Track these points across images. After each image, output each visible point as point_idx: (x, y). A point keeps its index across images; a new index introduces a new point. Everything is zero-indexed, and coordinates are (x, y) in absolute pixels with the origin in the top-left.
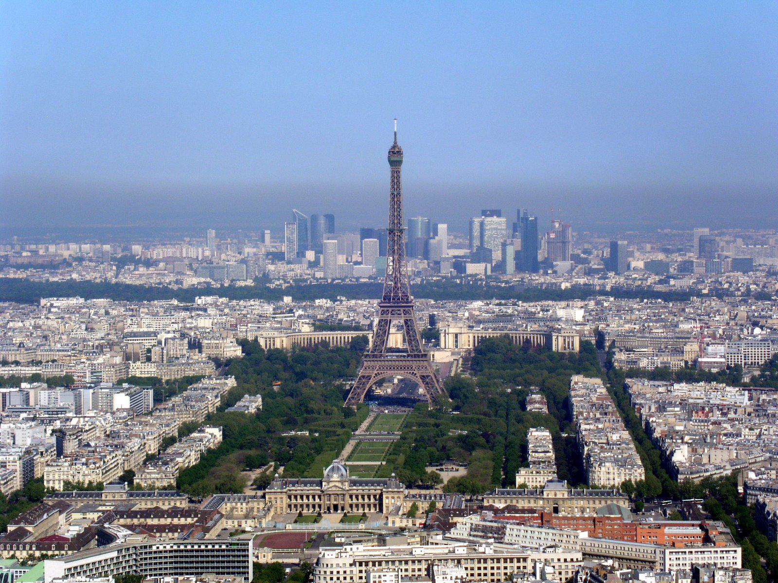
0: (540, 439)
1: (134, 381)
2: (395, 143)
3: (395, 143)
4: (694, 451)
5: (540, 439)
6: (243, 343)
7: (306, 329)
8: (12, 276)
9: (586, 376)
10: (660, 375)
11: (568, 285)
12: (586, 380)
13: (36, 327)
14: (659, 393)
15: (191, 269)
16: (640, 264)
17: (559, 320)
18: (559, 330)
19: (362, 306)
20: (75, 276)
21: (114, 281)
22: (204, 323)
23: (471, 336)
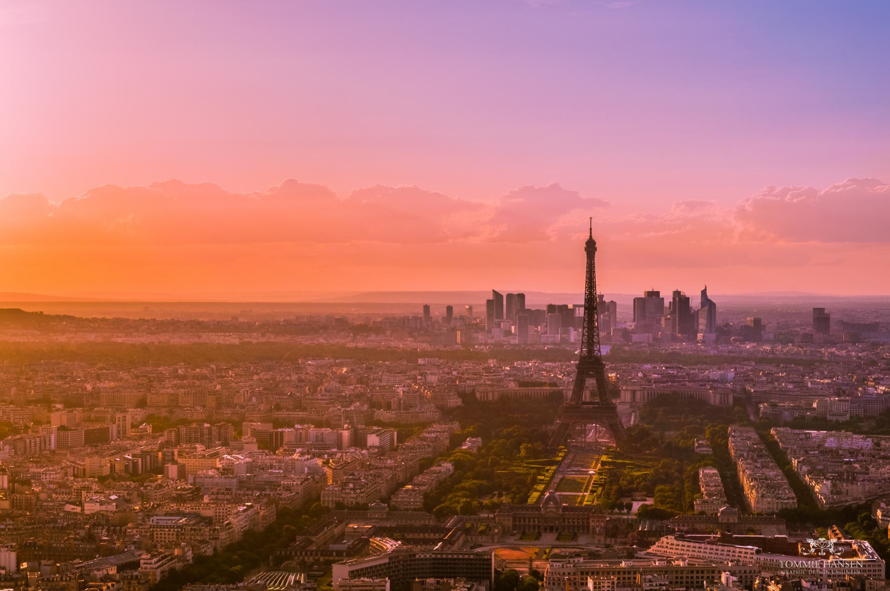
0: (708, 474)
1: (379, 423)
2: (591, 236)
3: (591, 236)
4: (834, 485)
5: (708, 474)
6: (462, 395)
7: (512, 385)
8: (272, 340)
9: (741, 426)
10: (800, 423)
11: (716, 352)
12: (742, 429)
13: (300, 380)
14: (801, 439)
15: (412, 336)
16: (771, 336)
17: (714, 381)
18: (715, 388)
19: (554, 367)
20: (322, 340)
21: (351, 345)
22: (433, 379)
23: (646, 392)
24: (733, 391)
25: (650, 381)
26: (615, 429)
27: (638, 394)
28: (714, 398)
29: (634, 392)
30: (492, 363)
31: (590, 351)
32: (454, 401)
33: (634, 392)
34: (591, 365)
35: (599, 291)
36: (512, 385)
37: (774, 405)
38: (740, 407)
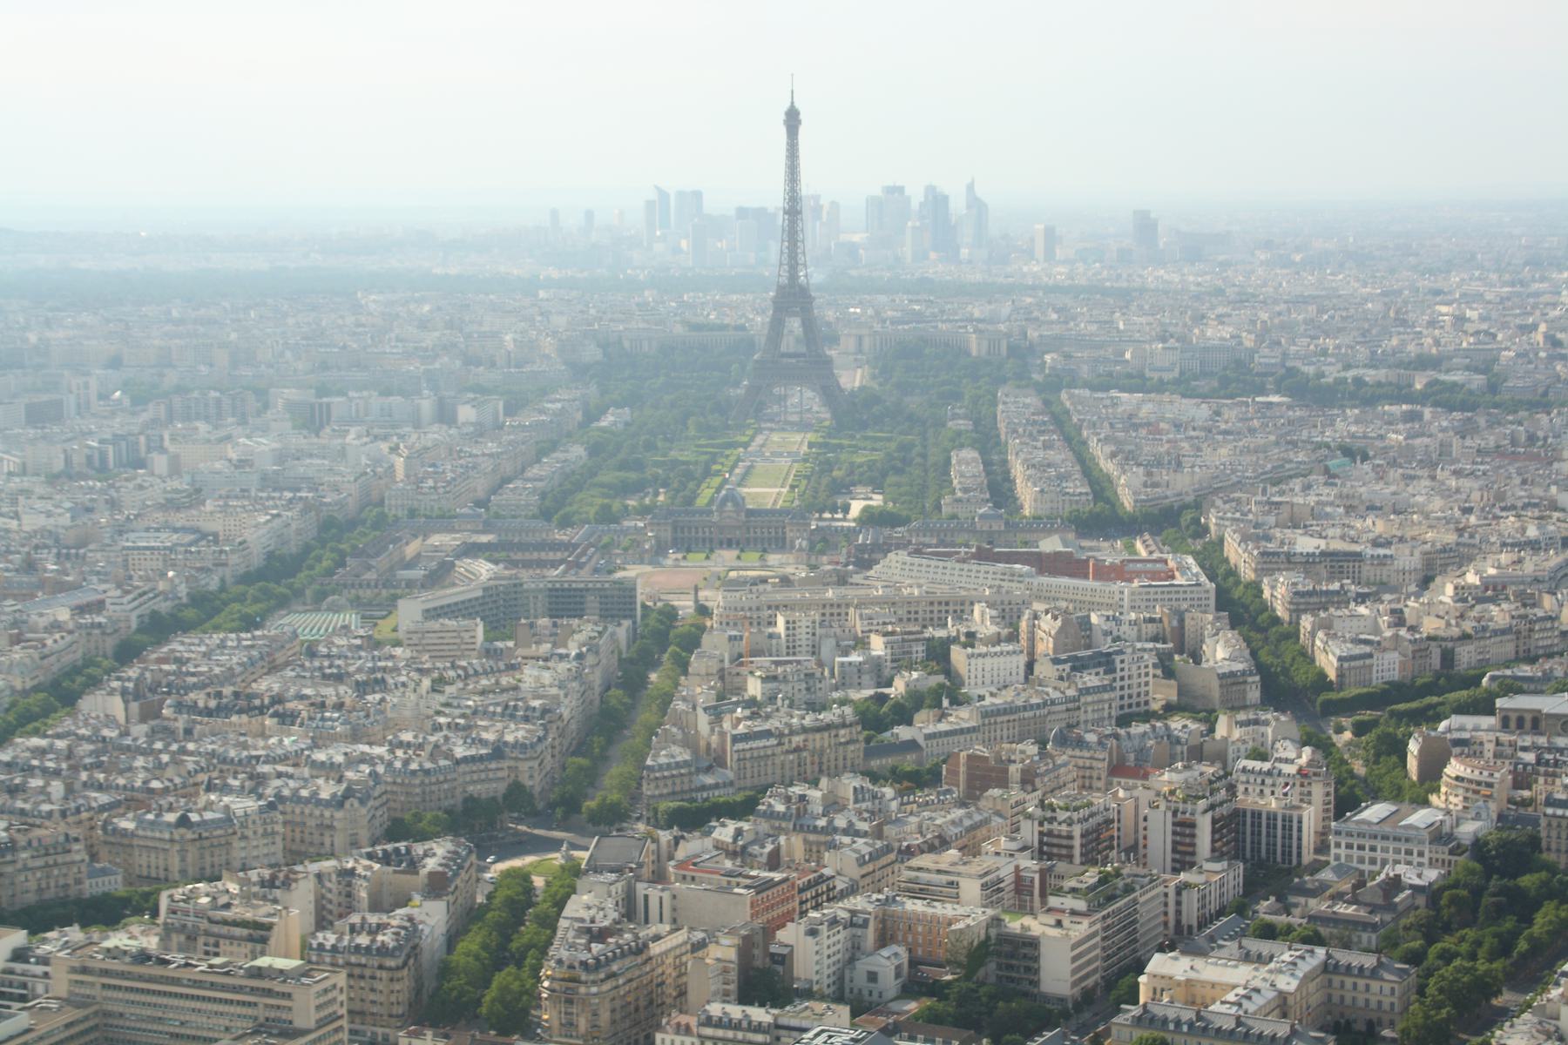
10: (1104, 383)
18: (981, 332)
21: (438, 271)
24: (1008, 335)
25: (884, 321)
26: (830, 392)
27: (867, 342)
28: (975, 346)
29: (860, 338)
30: (649, 295)
31: (793, 276)
32: (591, 353)
33: (860, 338)
34: (793, 297)
35: (809, 185)
36: (679, 330)
37: (1068, 356)
38: (1015, 361)
